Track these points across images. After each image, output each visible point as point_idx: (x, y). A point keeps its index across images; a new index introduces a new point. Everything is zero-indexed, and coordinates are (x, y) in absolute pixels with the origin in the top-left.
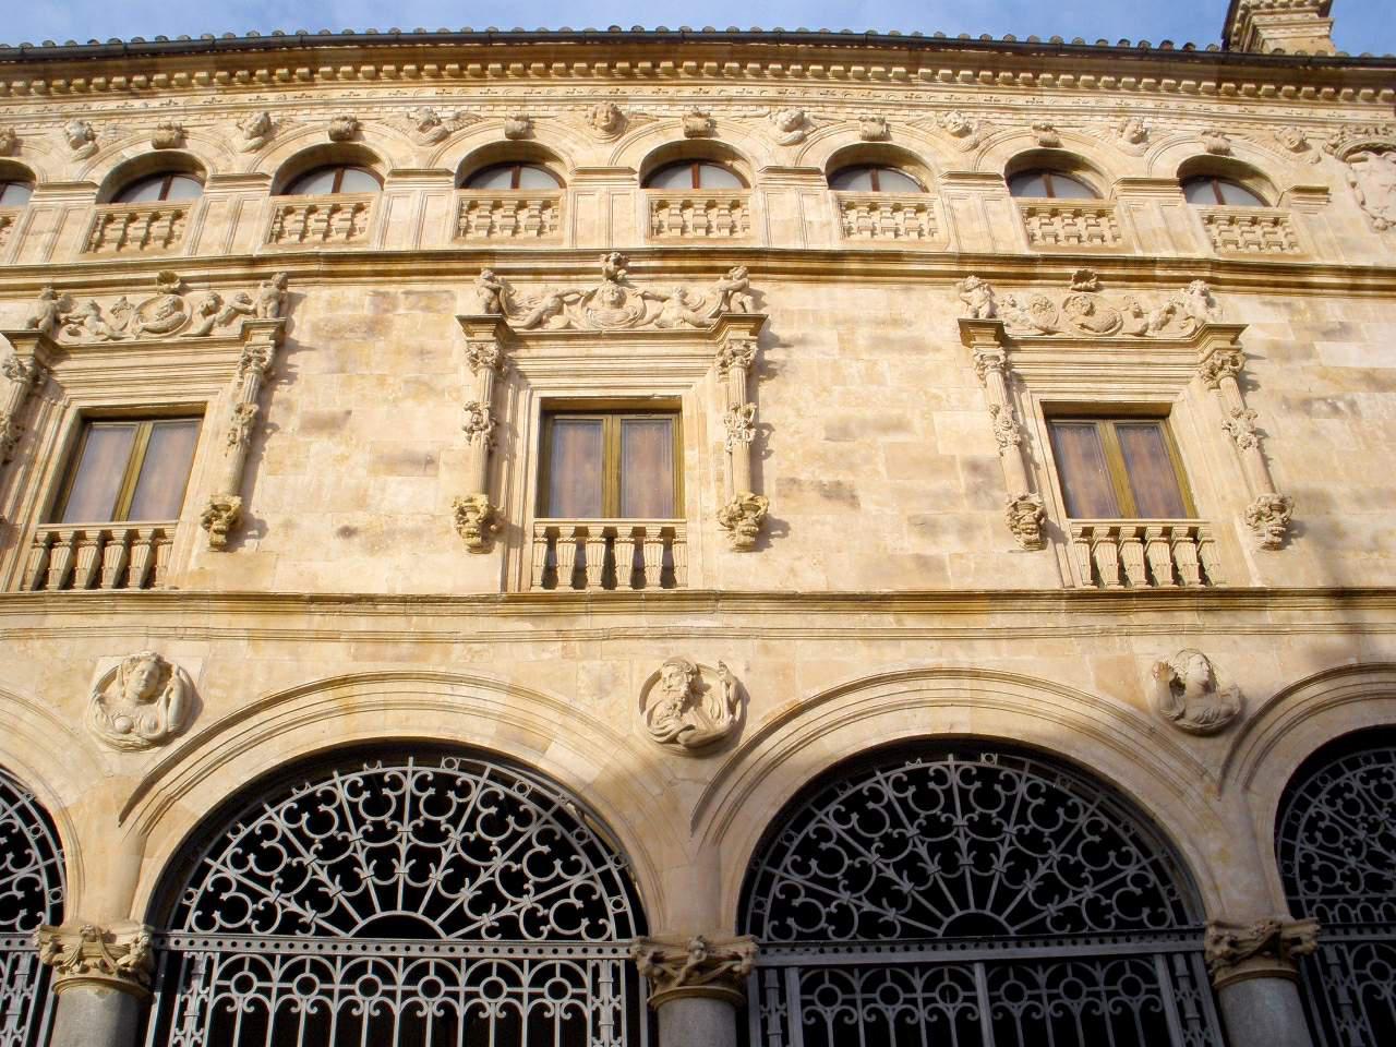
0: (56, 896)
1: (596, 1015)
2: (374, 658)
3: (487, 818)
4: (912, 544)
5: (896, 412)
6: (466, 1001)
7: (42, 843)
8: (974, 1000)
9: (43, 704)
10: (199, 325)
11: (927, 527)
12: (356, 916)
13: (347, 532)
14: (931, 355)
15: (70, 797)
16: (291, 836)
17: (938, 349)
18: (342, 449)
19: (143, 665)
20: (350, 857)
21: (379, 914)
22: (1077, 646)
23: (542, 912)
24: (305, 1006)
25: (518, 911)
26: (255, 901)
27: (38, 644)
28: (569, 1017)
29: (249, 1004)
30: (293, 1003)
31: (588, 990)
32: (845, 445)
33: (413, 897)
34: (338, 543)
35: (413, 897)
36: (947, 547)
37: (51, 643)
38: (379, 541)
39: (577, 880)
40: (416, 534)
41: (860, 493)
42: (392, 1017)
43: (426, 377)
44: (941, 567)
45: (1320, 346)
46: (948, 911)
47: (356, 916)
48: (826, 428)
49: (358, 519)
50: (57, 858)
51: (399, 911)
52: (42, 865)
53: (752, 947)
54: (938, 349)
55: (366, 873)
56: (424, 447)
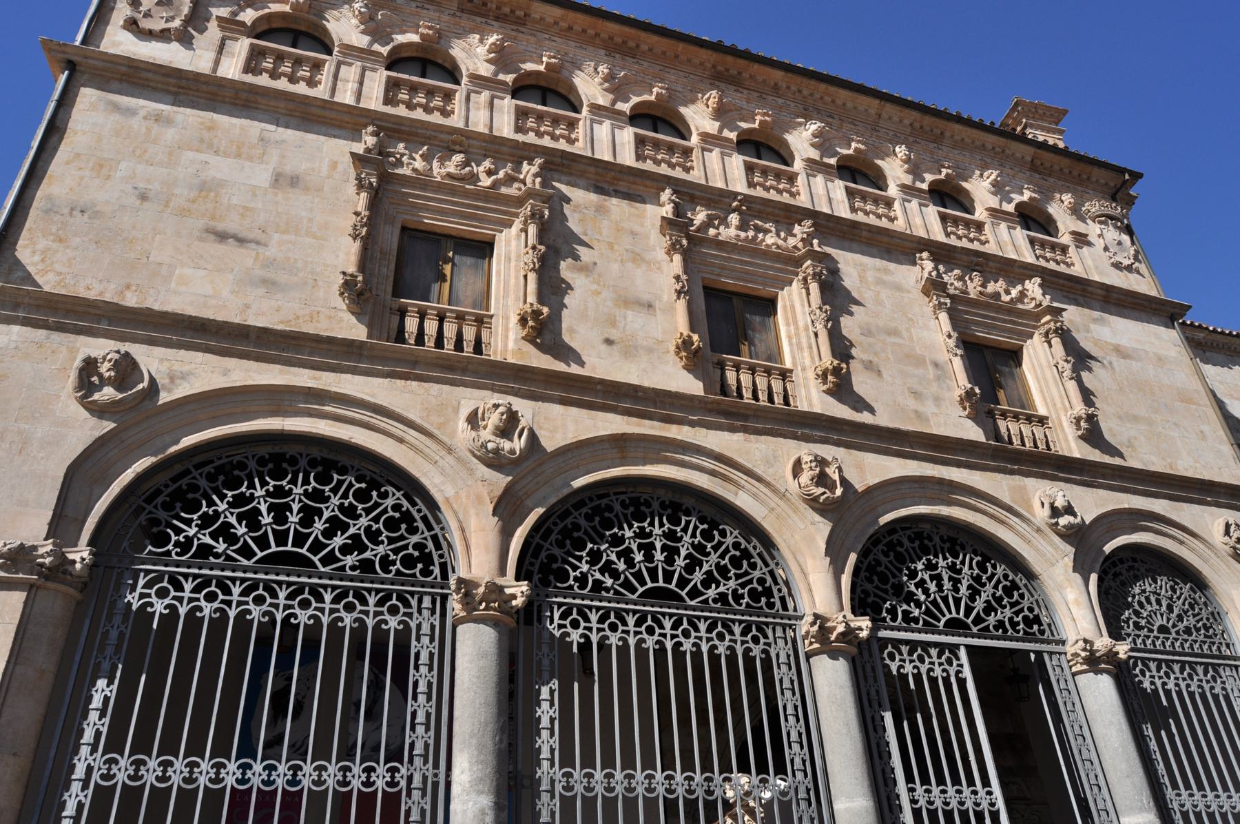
0: (441, 556)
1: (419, 626)
2: (639, 425)
3: (703, 530)
4: (911, 403)
5: (893, 324)
6: (374, 617)
7: (425, 519)
8: (961, 666)
9: (426, 425)
10: (486, 182)
11: (916, 394)
12: (687, 590)
13: (609, 342)
14: (905, 295)
15: (450, 491)
16: (724, 547)
17: (909, 292)
18: (594, 287)
19: (501, 409)
20: (254, 507)
21: (274, 549)
22: (999, 476)
23: (392, 557)
24: (303, 617)
25: (375, 556)
26: (574, 571)
27: (414, 383)
28: (582, 640)
29: (309, 618)
30: (607, 638)
31: (771, 639)
32: (871, 340)
33: (668, 577)
34: (604, 347)
35: (300, 540)
36: (928, 408)
37: (425, 385)
38: (630, 351)
39: (415, 539)
40: (650, 350)
41: (882, 369)
42: (321, 625)
43: (637, 250)
44: (928, 420)
45: (1092, 326)
46: (944, 615)
47: (687, 590)
48: (861, 328)
49: (614, 334)
50: (437, 530)
51: (289, 548)
52: (427, 534)
53: (869, 624)
54: (909, 292)
55: (319, 525)
56: (646, 297)
